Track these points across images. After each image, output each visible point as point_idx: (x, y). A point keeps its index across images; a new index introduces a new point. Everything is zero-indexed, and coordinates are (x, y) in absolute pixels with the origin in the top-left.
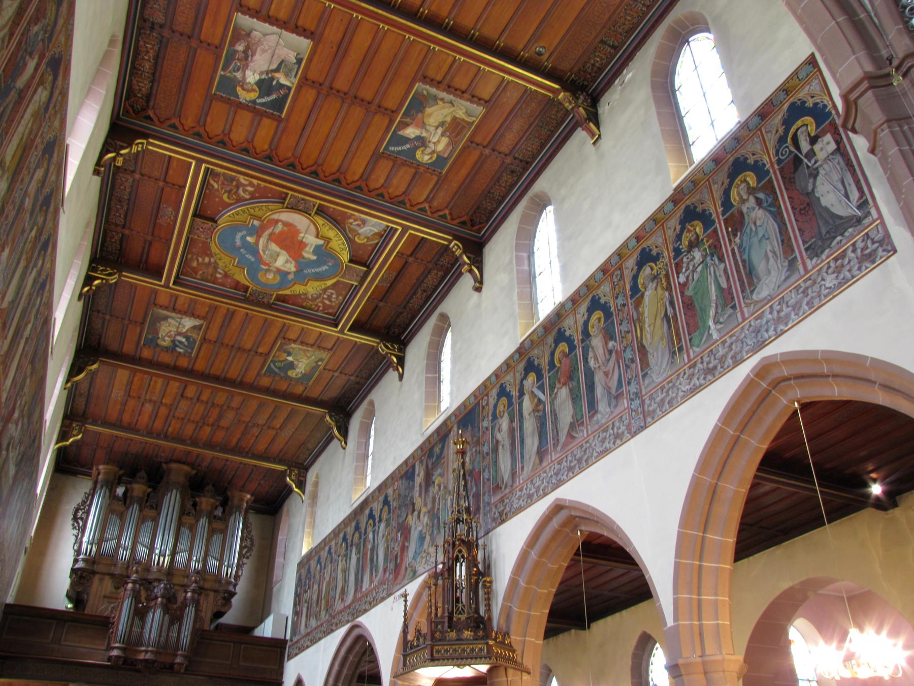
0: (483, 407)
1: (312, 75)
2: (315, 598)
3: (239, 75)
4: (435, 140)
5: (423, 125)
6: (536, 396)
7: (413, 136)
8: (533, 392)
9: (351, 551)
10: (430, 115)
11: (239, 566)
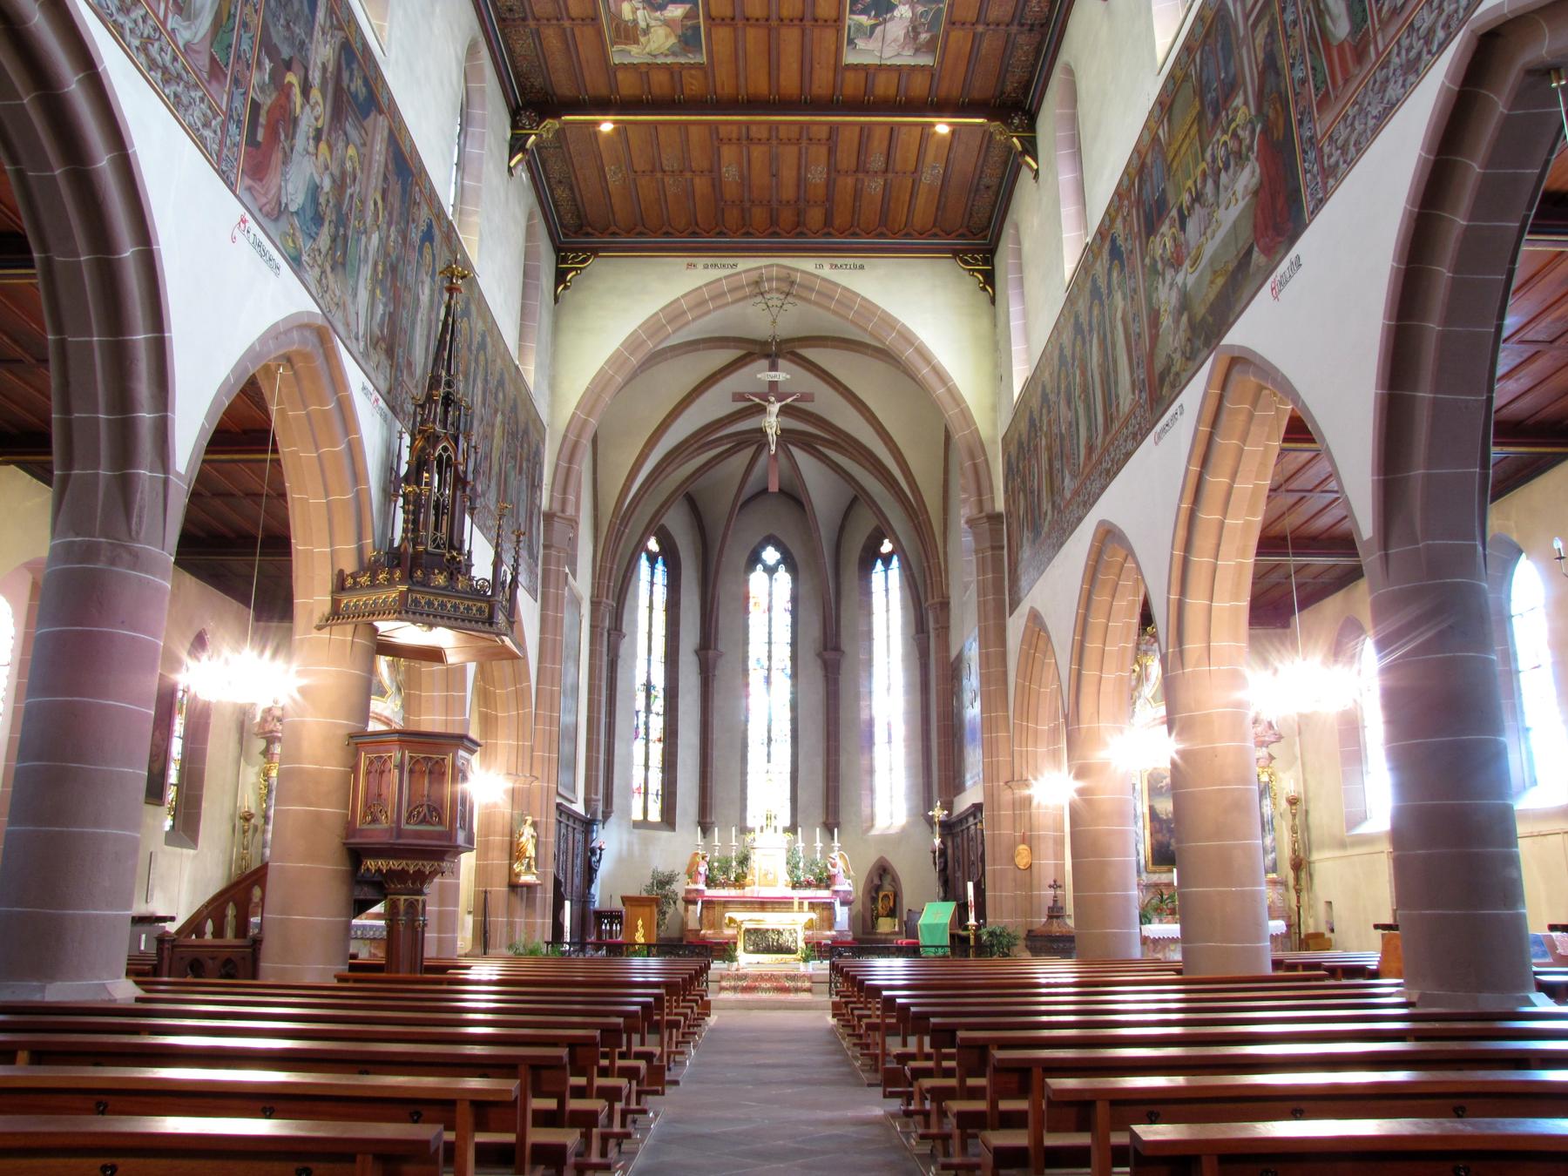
1: (829, 35)
3: (920, 9)
4: (640, 13)
5: (667, 23)
7: (671, 7)
10: (667, 37)
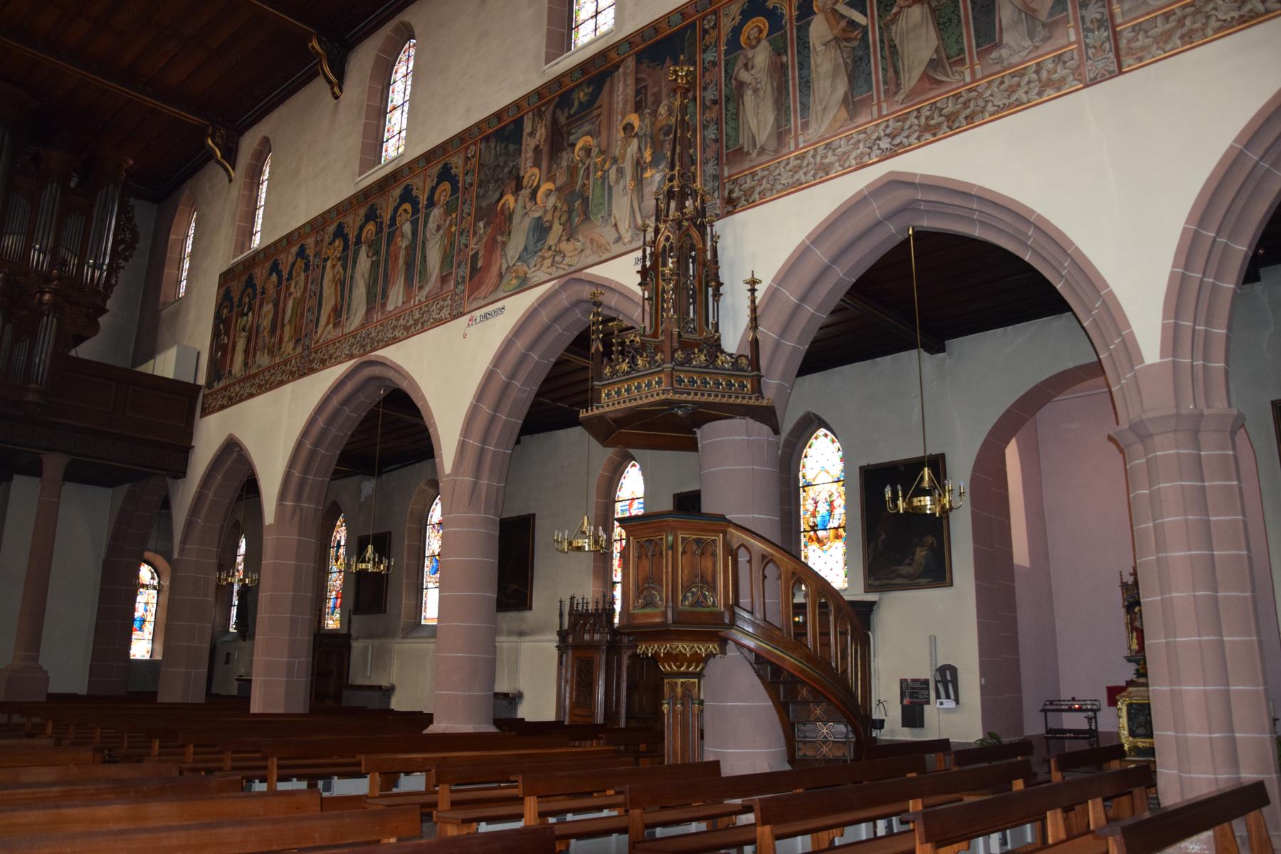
0: (705, 32)
2: (266, 323)
6: (843, 17)
8: (835, 11)
9: (357, 253)
11: (113, 269)
